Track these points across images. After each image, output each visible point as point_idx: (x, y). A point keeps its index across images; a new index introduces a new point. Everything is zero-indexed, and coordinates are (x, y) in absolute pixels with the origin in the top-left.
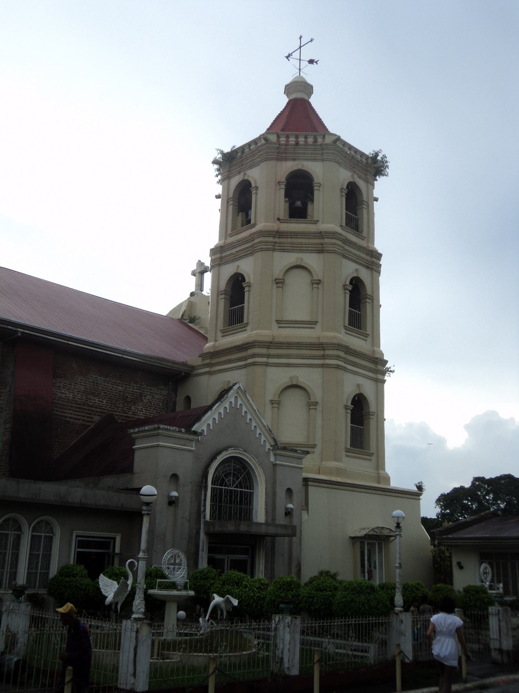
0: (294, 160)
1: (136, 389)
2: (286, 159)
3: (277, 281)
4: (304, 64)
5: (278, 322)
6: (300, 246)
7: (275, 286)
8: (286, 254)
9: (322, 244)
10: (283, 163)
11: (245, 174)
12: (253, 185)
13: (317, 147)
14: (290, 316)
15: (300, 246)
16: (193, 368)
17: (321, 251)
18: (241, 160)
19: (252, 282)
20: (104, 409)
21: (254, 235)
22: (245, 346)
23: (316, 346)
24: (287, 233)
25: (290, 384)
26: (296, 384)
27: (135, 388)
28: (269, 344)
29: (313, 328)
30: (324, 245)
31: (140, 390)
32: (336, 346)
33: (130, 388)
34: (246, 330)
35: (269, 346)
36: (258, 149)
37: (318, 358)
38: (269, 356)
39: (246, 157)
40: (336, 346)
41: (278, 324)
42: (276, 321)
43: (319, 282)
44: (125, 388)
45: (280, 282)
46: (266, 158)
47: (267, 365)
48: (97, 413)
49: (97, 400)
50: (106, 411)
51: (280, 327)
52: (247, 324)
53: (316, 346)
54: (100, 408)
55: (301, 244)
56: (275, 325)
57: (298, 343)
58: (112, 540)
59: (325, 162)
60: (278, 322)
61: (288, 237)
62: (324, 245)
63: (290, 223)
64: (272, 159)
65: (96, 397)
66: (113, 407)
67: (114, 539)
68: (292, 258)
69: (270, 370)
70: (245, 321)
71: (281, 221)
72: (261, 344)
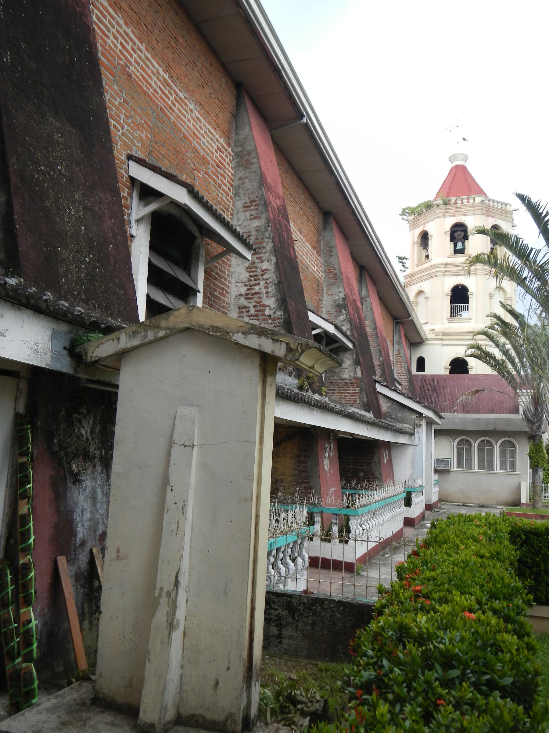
0: (493, 217)
16: (427, 339)
19: (475, 292)
64: (483, 214)
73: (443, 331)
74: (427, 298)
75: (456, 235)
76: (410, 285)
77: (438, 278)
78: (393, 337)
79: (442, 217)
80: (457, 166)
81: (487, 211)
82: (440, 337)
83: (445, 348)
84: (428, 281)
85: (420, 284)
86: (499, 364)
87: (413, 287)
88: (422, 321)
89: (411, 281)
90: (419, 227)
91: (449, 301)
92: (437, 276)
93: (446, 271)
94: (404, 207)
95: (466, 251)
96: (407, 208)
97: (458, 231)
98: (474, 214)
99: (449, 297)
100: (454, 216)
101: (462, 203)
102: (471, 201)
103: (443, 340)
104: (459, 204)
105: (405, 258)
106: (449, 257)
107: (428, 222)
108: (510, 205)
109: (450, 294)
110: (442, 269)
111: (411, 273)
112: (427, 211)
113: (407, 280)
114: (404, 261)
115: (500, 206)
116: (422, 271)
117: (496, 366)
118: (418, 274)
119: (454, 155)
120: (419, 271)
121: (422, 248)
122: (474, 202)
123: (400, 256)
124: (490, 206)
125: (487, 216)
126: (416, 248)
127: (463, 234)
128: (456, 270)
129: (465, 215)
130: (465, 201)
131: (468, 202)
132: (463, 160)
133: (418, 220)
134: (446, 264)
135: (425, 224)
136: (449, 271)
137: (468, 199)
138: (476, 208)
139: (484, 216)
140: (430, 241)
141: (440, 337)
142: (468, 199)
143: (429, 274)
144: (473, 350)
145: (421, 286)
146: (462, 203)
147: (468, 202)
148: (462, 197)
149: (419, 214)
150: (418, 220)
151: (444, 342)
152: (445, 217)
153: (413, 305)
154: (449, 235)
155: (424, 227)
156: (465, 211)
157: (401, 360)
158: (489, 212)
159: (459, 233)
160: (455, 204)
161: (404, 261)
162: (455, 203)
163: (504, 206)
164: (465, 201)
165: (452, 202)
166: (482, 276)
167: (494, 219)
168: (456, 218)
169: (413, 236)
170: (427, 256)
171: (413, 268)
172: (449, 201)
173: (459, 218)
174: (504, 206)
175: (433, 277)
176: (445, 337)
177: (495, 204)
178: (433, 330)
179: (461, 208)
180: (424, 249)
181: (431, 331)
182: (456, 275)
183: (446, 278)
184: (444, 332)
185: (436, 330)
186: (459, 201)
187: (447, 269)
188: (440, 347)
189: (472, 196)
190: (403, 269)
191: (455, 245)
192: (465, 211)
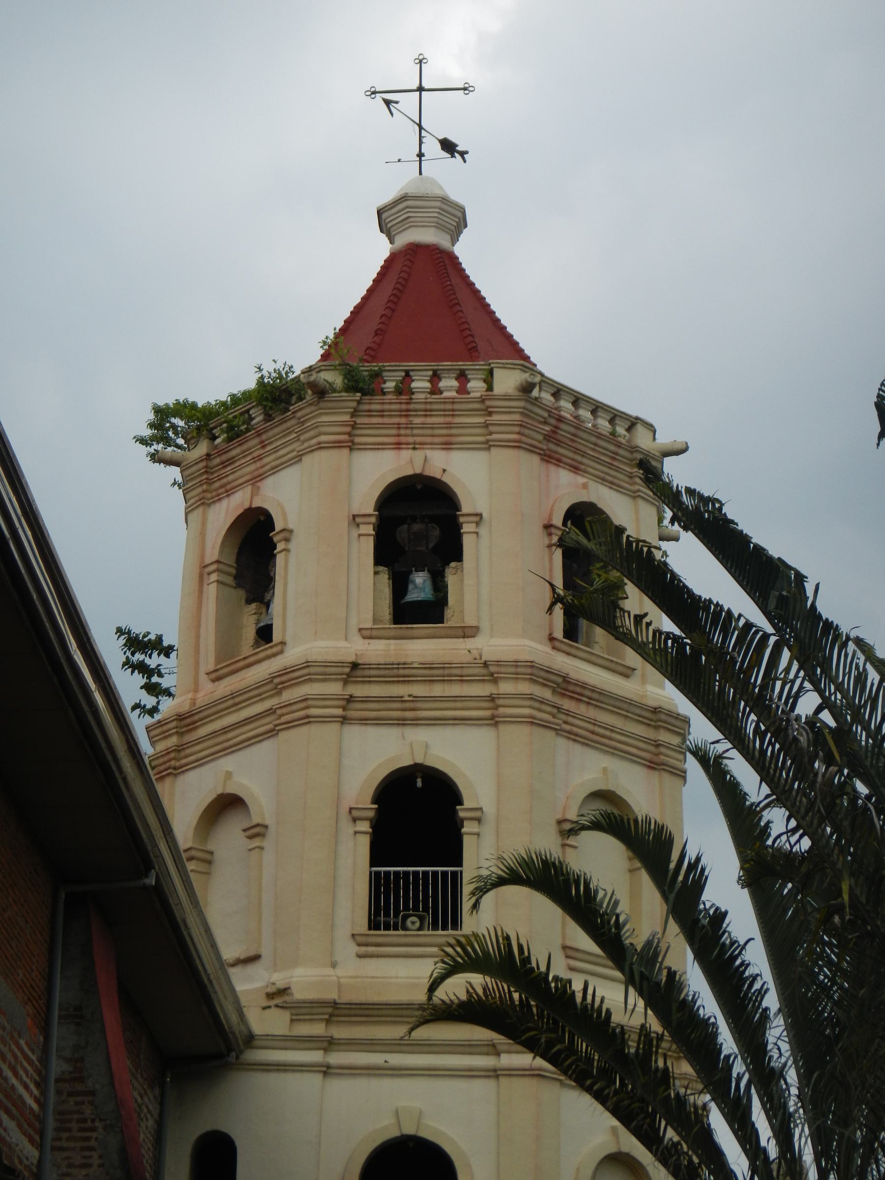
0: (576, 469)
4: (432, 148)
6: (608, 733)
9: (658, 746)
10: (552, 468)
13: (621, 452)
15: (608, 733)
16: (250, 1039)
17: (653, 765)
18: (404, 407)
19: (489, 809)
21: (503, 670)
24: (585, 688)
36: (488, 403)
39: (428, 407)
41: (567, 957)
46: (519, 441)
55: (612, 731)
59: (640, 502)
60: (571, 953)
61: (580, 700)
62: (662, 750)
63: (575, 656)
64: (531, 449)
71: (557, 644)
73: (333, 995)
74: (257, 832)
75: (402, 533)
76: (177, 771)
77: (315, 730)
78: (50, 979)
79: (337, 445)
80: (414, 250)
81: (548, 438)
82: (318, 1029)
83: (339, 1086)
84: (267, 746)
85: (227, 763)
86: (620, 1055)
87: (191, 777)
88: (228, 953)
89: (179, 749)
90: (229, 493)
91: (364, 844)
92: (307, 720)
93: (351, 699)
94: (167, 399)
95: (448, 613)
96: (185, 409)
97: (414, 519)
98: (488, 446)
99: (365, 826)
100: (398, 446)
101: (435, 390)
102: (476, 386)
103: (330, 1044)
104: (417, 396)
105: (158, 646)
106: (367, 635)
107: (275, 469)
108: (651, 428)
109: (369, 808)
110: (334, 688)
111: (186, 708)
112: (268, 417)
113: (161, 746)
114: (154, 661)
115: (603, 424)
116: (235, 700)
117: (606, 1074)
118: (219, 714)
119: (403, 198)
120: (223, 699)
121: (241, 594)
122: (490, 388)
123: (138, 629)
124: (560, 419)
125: (548, 458)
126: (212, 590)
127: (436, 533)
128: (400, 699)
129: (447, 446)
130: (449, 383)
131: (462, 390)
132: (440, 227)
133: (231, 461)
134: (355, 666)
135: (257, 479)
136: (366, 700)
137: (462, 377)
138: (495, 417)
139: (536, 459)
140: (280, 559)
141: (318, 1029)
142: (462, 377)
143: (271, 712)
144: (477, 980)
145: (229, 775)
146: (435, 390)
147: (462, 390)
148: (434, 365)
149: (234, 434)
150: (224, 464)
151: (336, 1058)
152: (352, 447)
153: (191, 866)
154: (370, 530)
155: (255, 492)
156: (449, 425)
157: (88, 1111)
158: (559, 443)
159: (416, 527)
160: (399, 391)
161: (154, 661)
162: (404, 389)
163: (621, 430)
164: (449, 383)
165: (390, 385)
166: (523, 732)
167: (581, 480)
168: (406, 454)
169: (203, 534)
170: (265, 634)
171: (196, 690)
172: (377, 375)
173: (419, 455)
174: (621, 430)
175: (290, 725)
176: (340, 1032)
177: (585, 413)
178: (283, 991)
179: (428, 412)
180: (249, 602)
181: (270, 996)
182: (402, 722)
183: (353, 732)
184: (335, 1004)
185: (299, 994)
186: (420, 384)
187: (358, 690)
188: (315, 1080)
189: (481, 365)
190: (149, 701)
191: (400, 586)
192: (449, 425)
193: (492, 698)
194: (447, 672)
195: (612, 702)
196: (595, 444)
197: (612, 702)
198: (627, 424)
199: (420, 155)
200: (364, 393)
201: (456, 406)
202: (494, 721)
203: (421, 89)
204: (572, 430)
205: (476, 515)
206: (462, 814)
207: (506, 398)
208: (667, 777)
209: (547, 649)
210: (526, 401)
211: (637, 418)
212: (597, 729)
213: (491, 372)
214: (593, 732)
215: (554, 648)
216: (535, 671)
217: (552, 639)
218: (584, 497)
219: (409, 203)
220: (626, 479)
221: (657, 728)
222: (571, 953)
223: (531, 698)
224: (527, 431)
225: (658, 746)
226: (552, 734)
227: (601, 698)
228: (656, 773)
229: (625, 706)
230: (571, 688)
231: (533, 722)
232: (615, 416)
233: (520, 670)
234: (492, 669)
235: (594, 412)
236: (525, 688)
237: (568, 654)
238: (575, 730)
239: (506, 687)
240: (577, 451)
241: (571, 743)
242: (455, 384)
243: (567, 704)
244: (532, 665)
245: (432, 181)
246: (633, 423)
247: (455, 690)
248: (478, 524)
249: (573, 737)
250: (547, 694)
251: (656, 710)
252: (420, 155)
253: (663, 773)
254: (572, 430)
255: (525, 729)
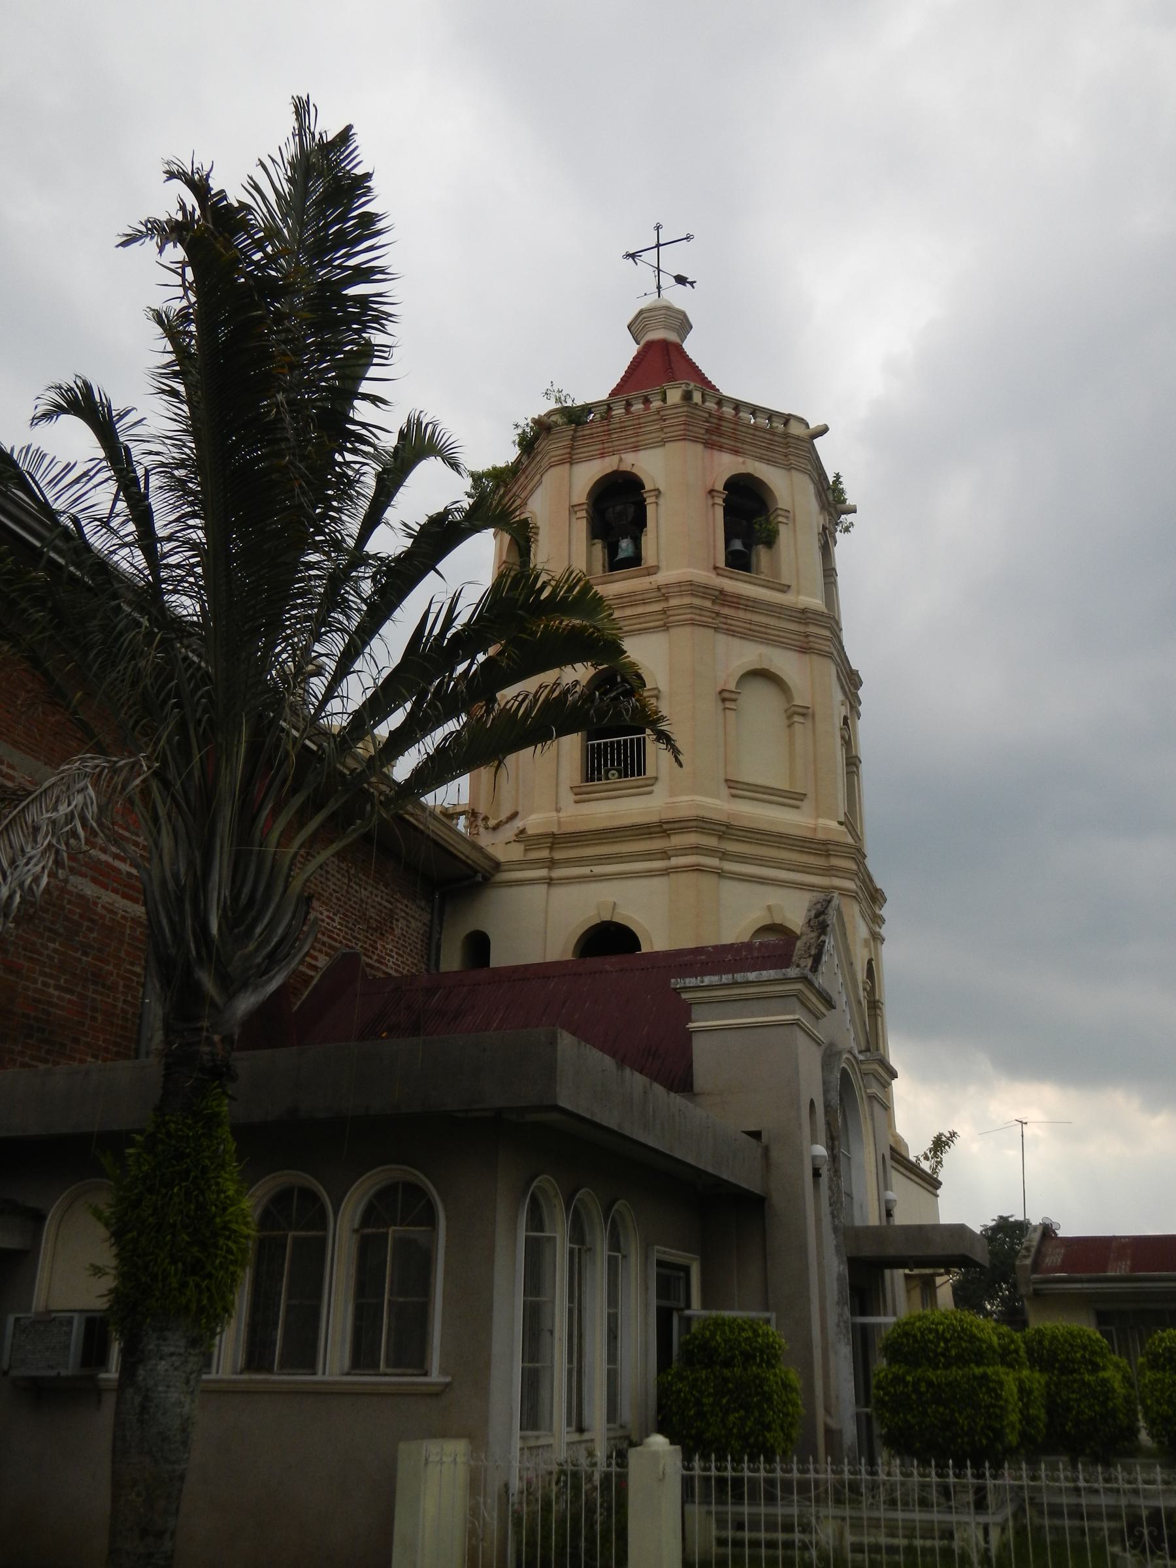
0: (736, 452)
1: (387, 901)
2: (721, 448)
3: (726, 695)
4: (667, 281)
5: (731, 783)
6: (763, 630)
7: (721, 706)
8: (736, 642)
9: (807, 636)
10: (716, 453)
11: (621, 460)
12: (648, 486)
13: (776, 438)
14: (751, 773)
15: (763, 630)
16: (497, 866)
17: (804, 650)
18: (606, 428)
19: (663, 686)
20: (335, 940)
21: (670, 590)
22: (665, 826)
23: (814, 846)
25: (768, 922)
26: (781, 925)
27: (385, 897)
28: (724, 828)
29: (797, 807)
30: (811, 639)
31: (392, 904)
32: (852, 851)
33: (376, 896)
34: (651, 793)
35: (724, 833)
36: (662, 413)
37: (819, 871)
38: (724, 856)
39: (622, 425)
40: (852, 851)
41: (730, 787)
42: (727, 781)
43: (805, 713)
44: (371, 893)
45: (726, 698)
46: (684, 435)
47: (721, 874)
48: (324, 949)
49: (326, 913)
50: (338, 945)
51: (734, 796)
52: (656, 779)
53: (814, 846)
54: (329, 937)
56: (725, 791)
57: (781, 836)
58: (682, 1274)
59: (794, 472)
60: (732, 784)
62: (811, 639)
63: (737, 580)
64: (695, 440)
65: (325, 907)
66: (349, 937)
67: (686, 1270)
68: (750, 655)
69: (727, 886)
70: (650, 772)
71: (721, 572)
72: (708, 826)
73: (555, 830)
79: (561, 463)
103: (552, 864)
125: (710, 445)
127: (631, 510)
129: (636, 448)
130: (638, 407)
142: (646, 401)
151: (557, 873)
152: (571, 462)
154: (584, 514)
167: (741, 459)
168: (607, 460)
184: (553, 835)
185: (530, 832)
191: (612, 549)
193: (664, 611)
194: (633, 598)
195: (764, 607)
196: (754, 435)
197: (764, 607)
198: (783, 421)
199: (659, 287)
200: (578, 424)
201: (642, 421)
202: (666, 627)
203: (658, 246)
204: (732, 426)
205: (655, 490)
206: (645, 694)
207: (675, 406)
208: (815, 657)
209: (713, 575)
210: (689, 406)
211: (790, 415)
212: (753, 627)
213: (665, 393)
214: (750, 630)
215: (718, 574)
216: (693, 588)
217: (715, 568)
218: (742, 470)
219: (644, 315)
220: (783, 458)
221: (806, 624)
222: (732, 784)
223: (691, 606)
224: (690, 428)
225: (807, 636)
226: (711, 631)
227: (756, 605)
228: (807, 656)
229: (778, 610)
230: (729, 599)
231: (693, 623)
232: (771, 415)
233: (683, 588)
234: (663, 591)
235: (753, 414)
236: (687, 600)
237: (731, 578)
238: (732, 628)
239: (673, 602)
240: (737, 440)
241: (730, 638)
242: (642, 406)
243: (726, 611)
244: (691, 583)
245: (667, 301)
246: (787, 419)
247: (640, 610)
248: (657, 497)
249: (732, 633)
250: (708, 604)
251: (804, 611)
252: (659, 287)
253: (812, 655)
254: (732, 426)
255: (688, 629)
